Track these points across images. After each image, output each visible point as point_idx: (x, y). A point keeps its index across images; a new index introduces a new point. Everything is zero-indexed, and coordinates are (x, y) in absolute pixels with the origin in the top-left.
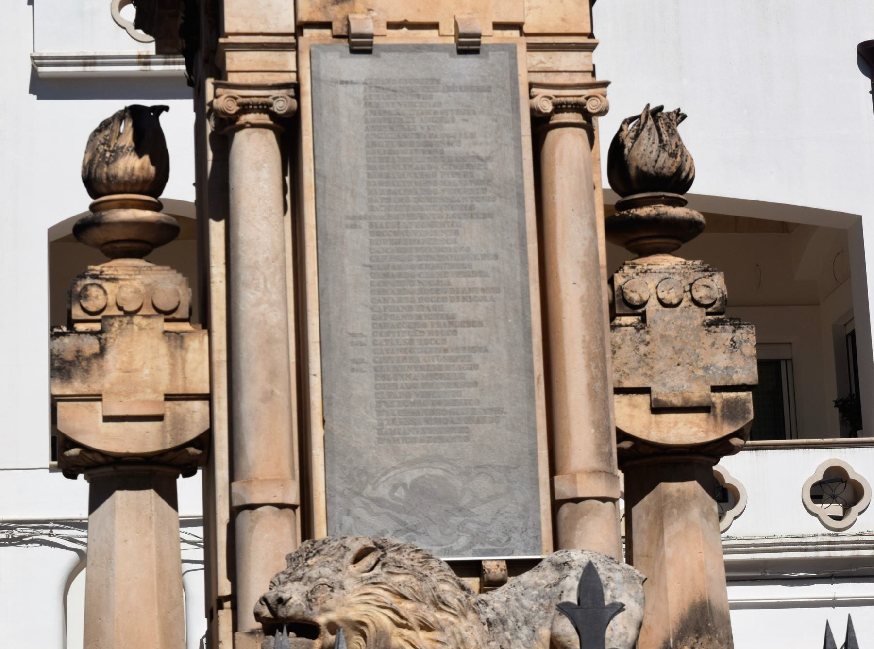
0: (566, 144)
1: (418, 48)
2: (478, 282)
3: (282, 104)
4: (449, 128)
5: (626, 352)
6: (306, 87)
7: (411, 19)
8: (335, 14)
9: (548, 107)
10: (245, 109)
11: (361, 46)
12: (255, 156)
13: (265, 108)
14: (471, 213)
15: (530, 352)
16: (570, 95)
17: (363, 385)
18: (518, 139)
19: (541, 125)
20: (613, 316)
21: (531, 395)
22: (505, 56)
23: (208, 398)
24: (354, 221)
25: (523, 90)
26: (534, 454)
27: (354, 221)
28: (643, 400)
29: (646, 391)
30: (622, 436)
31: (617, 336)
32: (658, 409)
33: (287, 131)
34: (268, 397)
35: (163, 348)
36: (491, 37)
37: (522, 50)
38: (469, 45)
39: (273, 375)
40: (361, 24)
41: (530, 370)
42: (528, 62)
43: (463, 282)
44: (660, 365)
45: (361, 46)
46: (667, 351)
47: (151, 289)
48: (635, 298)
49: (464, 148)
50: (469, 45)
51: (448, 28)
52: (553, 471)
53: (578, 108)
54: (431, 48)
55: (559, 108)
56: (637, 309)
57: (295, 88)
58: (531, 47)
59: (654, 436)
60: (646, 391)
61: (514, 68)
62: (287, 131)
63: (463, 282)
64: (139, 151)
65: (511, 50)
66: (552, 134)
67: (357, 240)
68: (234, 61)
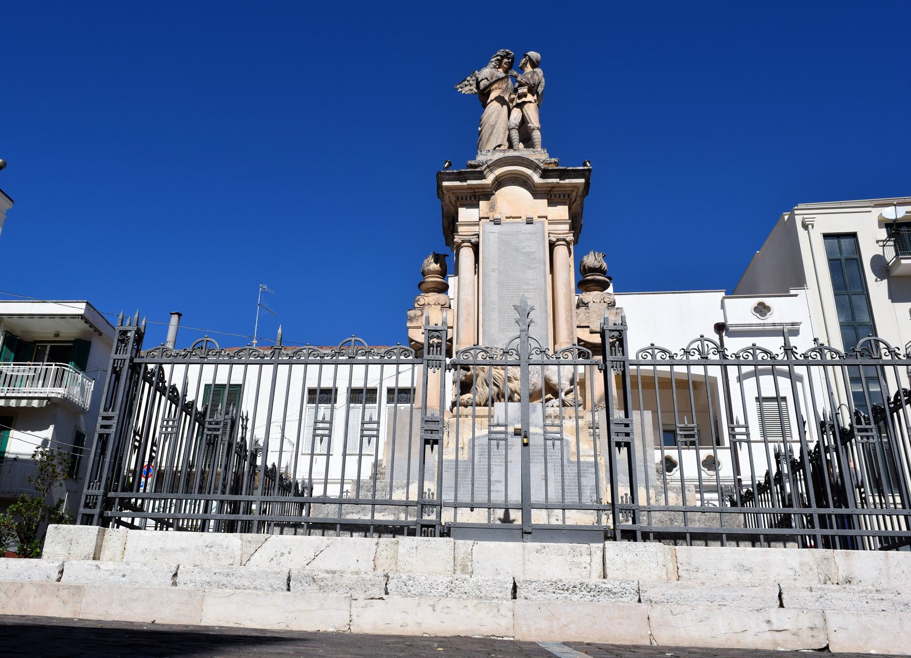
0: (561, 252)
1: (514, 223)
2: (531, 287)
3: (474, 239)
4: (523, 244)
5: (582, 316)
6: (481, 235)
7: (514, 215)
8: (490, 215)
9: (555, 240)
10: (463, 242)
11: (497, 222)
12: (466, 254)
13: (469, 241)
14: (529, 268)
15: (546, 306)
16: (561, 236)
17: (495, 315)
18: (544, 247)
19: (552, 245)
20: (578, 307)
21: (547, 318)
22: (541, 225)
23: (452, 328)
24: (494, 270)
25: (547, 235)
26: (547, 335)
27: (494, 270)
28: (587, 330)
29: (588, 327)
30: (579, 340)
31: (579, 311)
32: (592, 332)
33: (476, 247)
34: (467, 320)
35: (440, 313)
36: (535, 218)
37: (546, 222)
38: (530, 222)
39: (468, 314)
40: (497, 216)
41: (546, 312)
42: (548, 228)
43: (526, 287)
44: (592, 319)
45: (497, 222)
46: (595, 315)
47: (438, 299)
48: (586, 301)
49: (528, 250)
50: (530, 222)
51: (524, 218)
52: (555, 343)
53: (564, 240)
54: (518, 223)
55: (558, 240)
56: (586, 305)
57: (478, 235)
58: (549, 224)
59: (591, 340)
60: (588, 327)
61: (543, 227)
62: (476, 247)
63: (526, 287)
64: (436, 262)
65: (543, 223)
66: (556, 248)
67: (494, 276)
68: (460, 229)
